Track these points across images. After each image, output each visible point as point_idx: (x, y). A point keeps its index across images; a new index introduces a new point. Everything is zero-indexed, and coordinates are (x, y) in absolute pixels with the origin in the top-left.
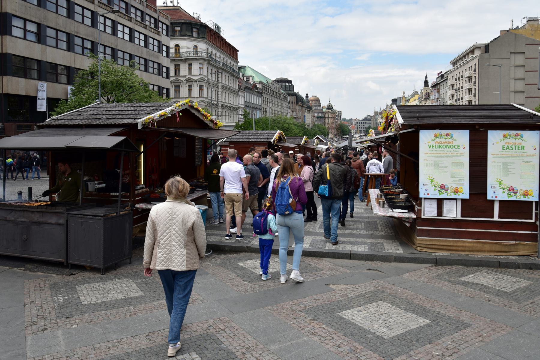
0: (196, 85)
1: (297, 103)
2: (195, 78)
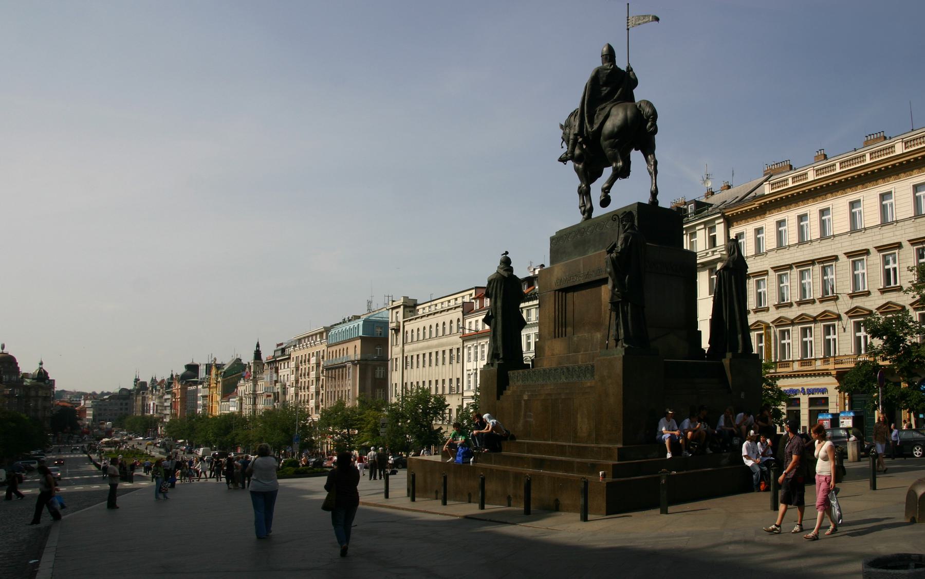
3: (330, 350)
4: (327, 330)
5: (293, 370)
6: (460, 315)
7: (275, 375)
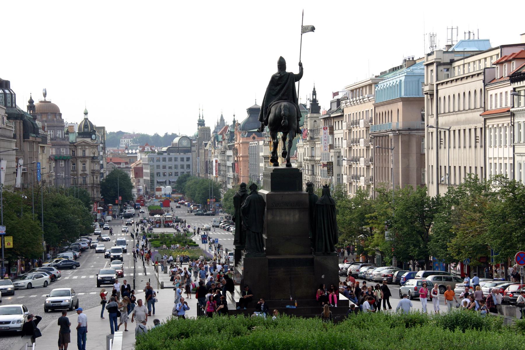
1: (26, 136)
3: (380, 110)
4: (374, 82)
5: (346, 133)
6: (481, 85)
7: (330, 137)
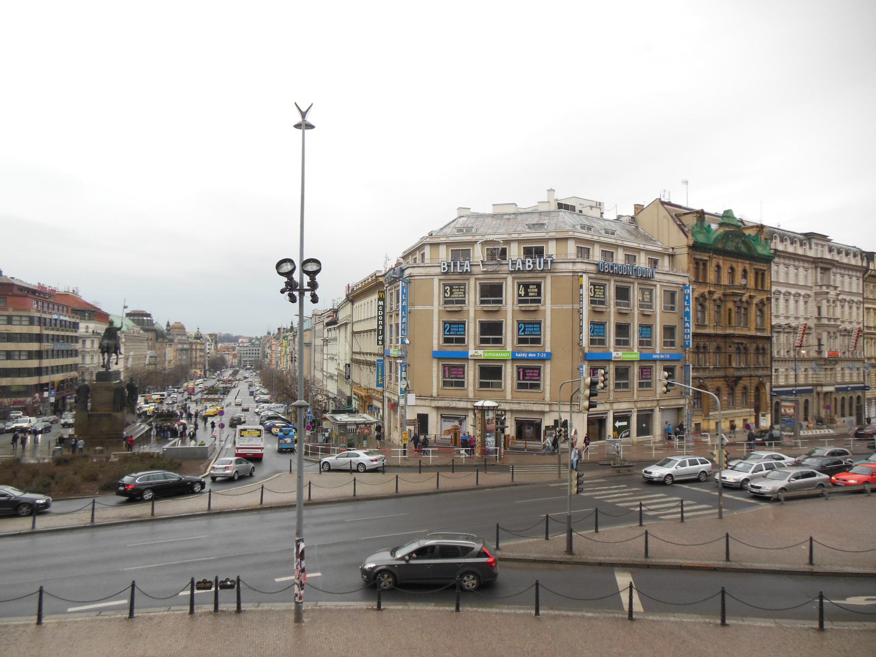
0: (88, 355)
1: (157, 339)
2: (87, 350)
